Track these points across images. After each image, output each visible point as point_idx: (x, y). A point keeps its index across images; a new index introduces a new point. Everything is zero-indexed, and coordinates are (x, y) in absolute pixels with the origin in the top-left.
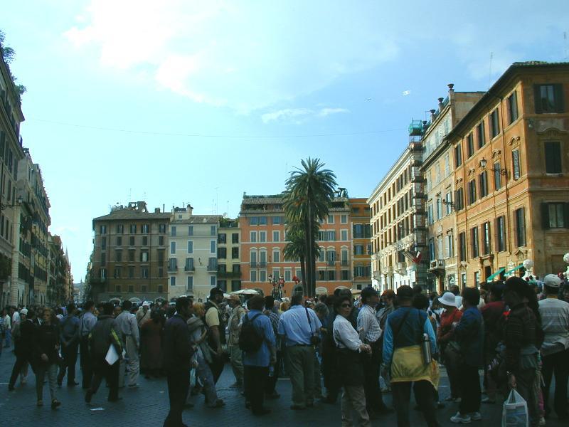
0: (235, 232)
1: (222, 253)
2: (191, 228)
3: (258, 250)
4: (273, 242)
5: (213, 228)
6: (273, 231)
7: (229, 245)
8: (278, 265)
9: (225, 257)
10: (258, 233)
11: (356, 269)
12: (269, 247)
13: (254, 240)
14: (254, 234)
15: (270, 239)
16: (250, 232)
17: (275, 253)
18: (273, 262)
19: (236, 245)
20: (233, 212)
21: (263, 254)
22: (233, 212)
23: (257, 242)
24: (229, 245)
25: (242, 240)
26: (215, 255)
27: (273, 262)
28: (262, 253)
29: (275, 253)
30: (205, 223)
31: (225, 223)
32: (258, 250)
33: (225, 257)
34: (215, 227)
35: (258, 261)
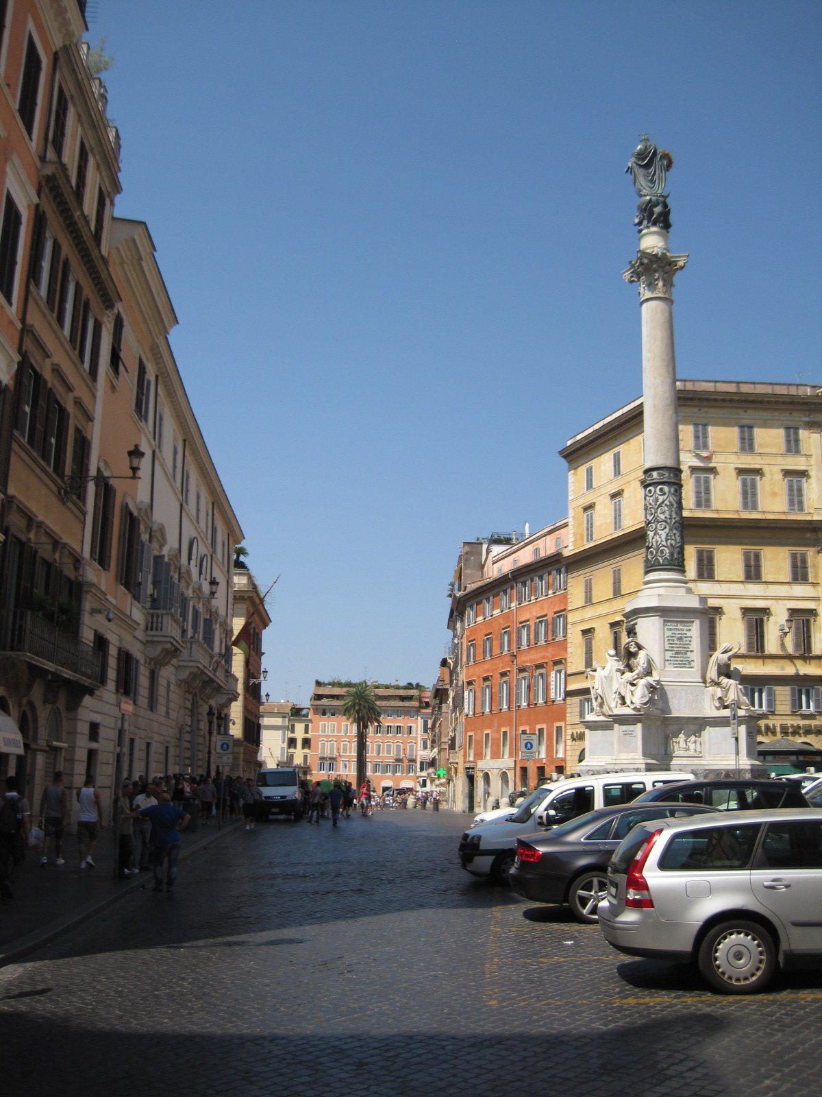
1: (292, 742)
8: (346, 757)
9: (295, 748)
11: (422, 764)
15: (339, 730)
16: (320, 723)
19: (307, 736)
20: (305, 702)
22: (305, 702)
24: (299, 733)
26: (285, 745)
31: (297, 712)
33: (295, 748)
35: (327, 754)
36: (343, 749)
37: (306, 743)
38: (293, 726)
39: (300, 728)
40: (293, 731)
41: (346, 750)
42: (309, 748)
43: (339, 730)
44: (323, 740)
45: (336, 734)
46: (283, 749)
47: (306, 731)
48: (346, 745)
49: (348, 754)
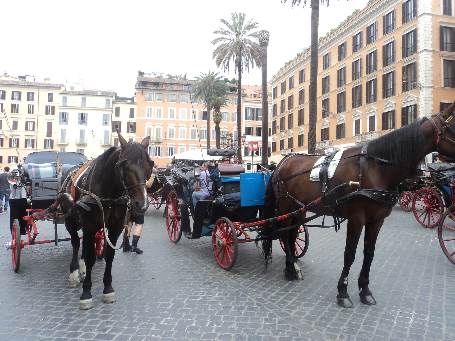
0: (132, 106)
1: (117, 127)
2: (84, 100)
3: (154, 126)
4: (169, 119)
5: (108, 101)
6: (169, 109)
7: (124, 118)
8: (172, 141)
10: (154, 109)
12: (165, 124)
13: (150, 115)
14: (150, 110)
15: (165, 116)
17: (170, 129)
18: (168, 138)
19: (132, 120)
21: (158, 130)
23: (152, 118)
24: (124, 118)
25: (137, 116)
26: (109, 128)
27: (168, 138)
28: (157, 129)
29: (170, 129)
30: (99, 95)
32: (154, 126)
34: (109, 100)
36: (170, 134)
37: (132, 127)
38: (118, 110)
39: (125, 109)
40: (117, 114)
41: (173, 135)
42: (134, 132)
43: (165, 116)
44: (149, 125)
45: (162, 118)
46: (106, 132)
47: (132, 115)
48: (173, 129)
49: (174, 139)
